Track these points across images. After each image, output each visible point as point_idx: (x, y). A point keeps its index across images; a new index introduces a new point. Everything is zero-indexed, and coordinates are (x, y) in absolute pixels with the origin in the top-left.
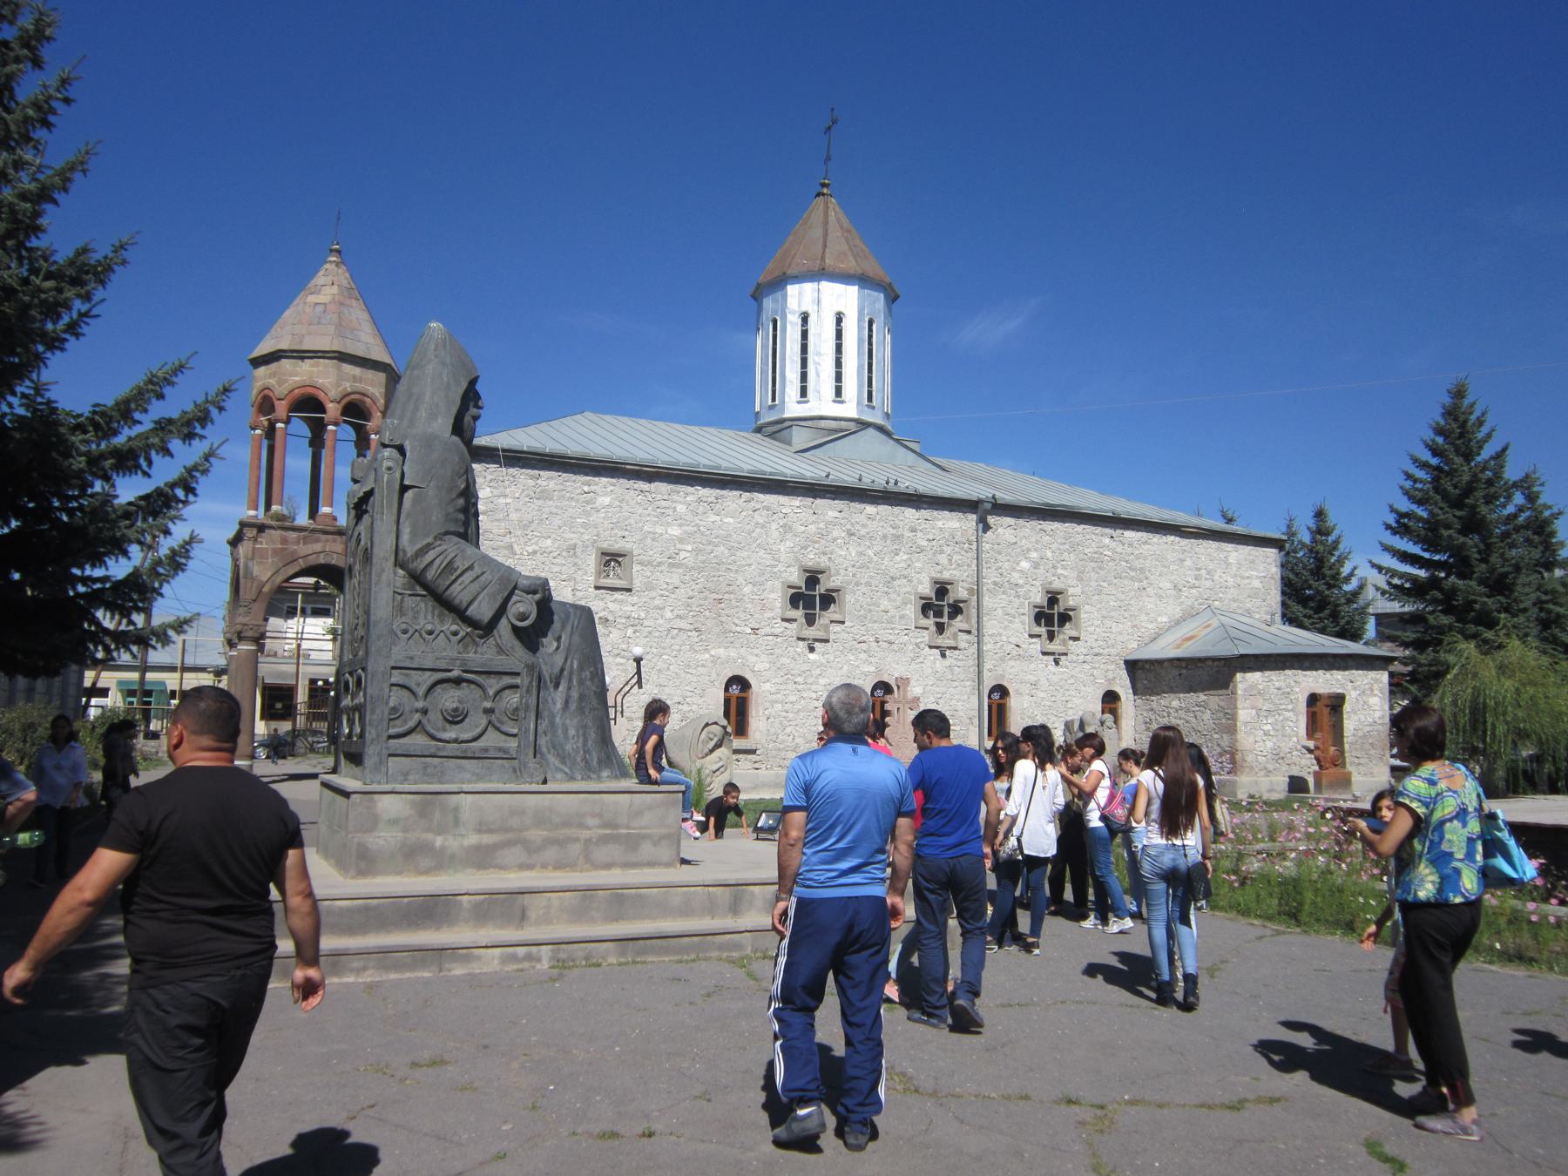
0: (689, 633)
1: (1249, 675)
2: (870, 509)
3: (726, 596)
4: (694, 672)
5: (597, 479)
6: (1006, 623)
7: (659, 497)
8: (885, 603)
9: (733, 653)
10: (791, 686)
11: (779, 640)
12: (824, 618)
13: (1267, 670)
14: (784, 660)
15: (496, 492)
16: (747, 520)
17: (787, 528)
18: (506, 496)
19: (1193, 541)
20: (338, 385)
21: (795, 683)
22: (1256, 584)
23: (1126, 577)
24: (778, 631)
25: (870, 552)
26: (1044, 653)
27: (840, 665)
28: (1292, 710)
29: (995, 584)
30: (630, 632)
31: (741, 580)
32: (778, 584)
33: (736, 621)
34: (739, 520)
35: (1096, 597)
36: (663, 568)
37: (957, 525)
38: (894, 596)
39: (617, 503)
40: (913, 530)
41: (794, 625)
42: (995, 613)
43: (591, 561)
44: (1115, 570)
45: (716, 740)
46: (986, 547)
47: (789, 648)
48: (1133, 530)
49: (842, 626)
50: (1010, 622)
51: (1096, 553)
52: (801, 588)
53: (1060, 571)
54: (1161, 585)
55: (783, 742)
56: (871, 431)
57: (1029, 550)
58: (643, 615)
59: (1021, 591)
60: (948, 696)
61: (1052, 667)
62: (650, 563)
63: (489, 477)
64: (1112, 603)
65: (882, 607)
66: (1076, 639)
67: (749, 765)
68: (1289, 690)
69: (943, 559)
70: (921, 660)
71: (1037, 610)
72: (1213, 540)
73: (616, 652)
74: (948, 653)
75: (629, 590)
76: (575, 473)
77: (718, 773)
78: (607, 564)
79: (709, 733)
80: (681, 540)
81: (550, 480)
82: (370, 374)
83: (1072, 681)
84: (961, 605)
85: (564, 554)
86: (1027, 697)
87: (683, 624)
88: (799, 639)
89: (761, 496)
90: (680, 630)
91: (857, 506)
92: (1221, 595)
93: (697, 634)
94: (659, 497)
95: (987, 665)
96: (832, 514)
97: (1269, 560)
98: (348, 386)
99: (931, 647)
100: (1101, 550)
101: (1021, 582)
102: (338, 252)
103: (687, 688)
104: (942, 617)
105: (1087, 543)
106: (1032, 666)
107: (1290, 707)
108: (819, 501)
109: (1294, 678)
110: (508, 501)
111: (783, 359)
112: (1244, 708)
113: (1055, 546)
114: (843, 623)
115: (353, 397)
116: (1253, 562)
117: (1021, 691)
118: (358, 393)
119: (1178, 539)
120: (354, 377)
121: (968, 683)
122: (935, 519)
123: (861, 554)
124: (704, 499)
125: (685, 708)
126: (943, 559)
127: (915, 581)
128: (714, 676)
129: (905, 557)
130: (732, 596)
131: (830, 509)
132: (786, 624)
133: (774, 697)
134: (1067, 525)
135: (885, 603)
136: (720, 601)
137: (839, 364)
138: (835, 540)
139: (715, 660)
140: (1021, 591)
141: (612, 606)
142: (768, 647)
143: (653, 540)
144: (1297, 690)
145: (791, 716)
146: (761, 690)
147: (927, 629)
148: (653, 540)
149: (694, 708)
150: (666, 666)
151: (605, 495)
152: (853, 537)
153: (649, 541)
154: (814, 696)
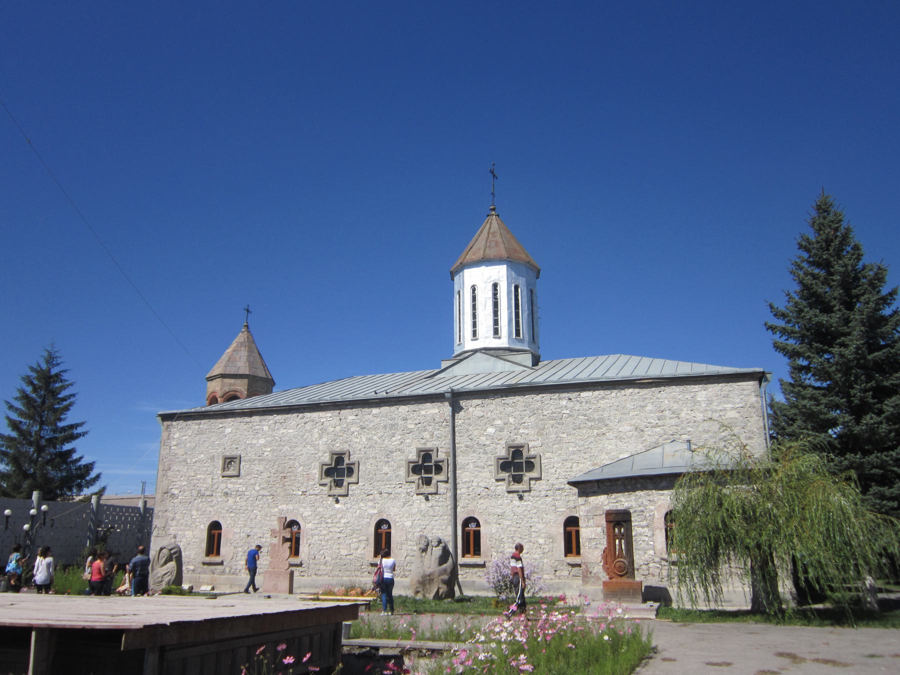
0: (268, 497)
1: (592, 499)
2: (375, 411)
3: (288, 474)
5: (225, 420)
6: (476, 473)
7: (255, 424)
8: (386, 469)
9: (291, 507)
10: (324, 525)
12: (347, 480)
13: (613, 493)
14: (321, 509)
15: (182, 434)
16: (301, 430)
17: (323, 431)
18: (185, 436)
19: (653, 389)
20: (221, 389)
21: (327, 523)
22: (732, 414)
23: (584, 427)
24: (316, 492)
25: (375, 438)
26: (509, 492)
27: (354, 511)
28: (647, 526)
29: (467, 446)
30: (238, 498)
31: (297, 464)
33: (293, 488)
34: (296, 430)
35: (555, 446)
36: (256, 462)
37: (437, 411)
38: (393, 463)
39: (234, 431)
40: (405, 419)
41: (326, 488)
42: (467, 467)
43: (220, 463)
46: (458, 422)
47: (324, 502)
48: (590, 390)
49: (357, 486)
50: (480, 472)
51: (555, 413)
52: (331, 465)
53: (521, 431)
54: (620, 429)
55: (318, 559)
56: (478, 354)
57: (494, 419)
59: (488, 449)
60: (430, 527)
61: (517, 502)
62: (249, 461)
63: (179, 427)
64: (570, 449)
65: (384, 471)
66: (540, 479)
68: (642, 508)
69: (426, 435)
70: (410, 503)
71: (501, 461)
72: (677, 385)
73: (230, 510)
74: (430, 497)
75: (238, 476)
76: (216, 419)
77: (166, 576)
78: (230, 463)
80: (265, 446)
81: (205, 424)
82: (238, 381)
83: (535, 511)
84: (441, 464)
85: (209, 461)
86: (495, 525)
87: (266, 493)
88: (330, 496)
89: (308, 415)
90: (263, 496)
91: (366, 410)
92: (690, 429)
93: (271, 497)
94: (255, 424)
95: (460, 504)
96: (351, 418)
97: (745, 392)
98: (227, 389)
99: (418, 494)
100: (560, 410)
101: (488, 443)
102: (247, 326)
104: (431, 473)
106: (500, 502)
107: (644, 523)
108: (343, 412)
109: (648, 498)
110: (187, 437)
111: (463, 319)
112: (587, 526)
113: (517, 413)
114: (357, 483)
115: (230, 393)
116: (727, 396)
117: (490, 521)
118: (232, 391)
119: (637, 390)
120: (230, 385)
121: (446, 517)
123: (369, 439)
124: (278, 421)
127: (406, 451)
129: (399, 437)
130: (292, 474)
131: (349, 415)
132: (321, 488)
133: (313, 532)
134: (526, 397)
135: (386, 469)
136: (285, 477)
137: (496, 313)
138: (353, 433)
140: (488, 449)
141: (230, 486)
142: (311, 502)
143: (251, 447)
144: (652, 508)
145: (323, 543)
146: (306, 527)
147: (414, 482)
148: (251, 447)
150: (255, 516)
151: (229, 428)
153: (249, 448)
154: (338, 530)
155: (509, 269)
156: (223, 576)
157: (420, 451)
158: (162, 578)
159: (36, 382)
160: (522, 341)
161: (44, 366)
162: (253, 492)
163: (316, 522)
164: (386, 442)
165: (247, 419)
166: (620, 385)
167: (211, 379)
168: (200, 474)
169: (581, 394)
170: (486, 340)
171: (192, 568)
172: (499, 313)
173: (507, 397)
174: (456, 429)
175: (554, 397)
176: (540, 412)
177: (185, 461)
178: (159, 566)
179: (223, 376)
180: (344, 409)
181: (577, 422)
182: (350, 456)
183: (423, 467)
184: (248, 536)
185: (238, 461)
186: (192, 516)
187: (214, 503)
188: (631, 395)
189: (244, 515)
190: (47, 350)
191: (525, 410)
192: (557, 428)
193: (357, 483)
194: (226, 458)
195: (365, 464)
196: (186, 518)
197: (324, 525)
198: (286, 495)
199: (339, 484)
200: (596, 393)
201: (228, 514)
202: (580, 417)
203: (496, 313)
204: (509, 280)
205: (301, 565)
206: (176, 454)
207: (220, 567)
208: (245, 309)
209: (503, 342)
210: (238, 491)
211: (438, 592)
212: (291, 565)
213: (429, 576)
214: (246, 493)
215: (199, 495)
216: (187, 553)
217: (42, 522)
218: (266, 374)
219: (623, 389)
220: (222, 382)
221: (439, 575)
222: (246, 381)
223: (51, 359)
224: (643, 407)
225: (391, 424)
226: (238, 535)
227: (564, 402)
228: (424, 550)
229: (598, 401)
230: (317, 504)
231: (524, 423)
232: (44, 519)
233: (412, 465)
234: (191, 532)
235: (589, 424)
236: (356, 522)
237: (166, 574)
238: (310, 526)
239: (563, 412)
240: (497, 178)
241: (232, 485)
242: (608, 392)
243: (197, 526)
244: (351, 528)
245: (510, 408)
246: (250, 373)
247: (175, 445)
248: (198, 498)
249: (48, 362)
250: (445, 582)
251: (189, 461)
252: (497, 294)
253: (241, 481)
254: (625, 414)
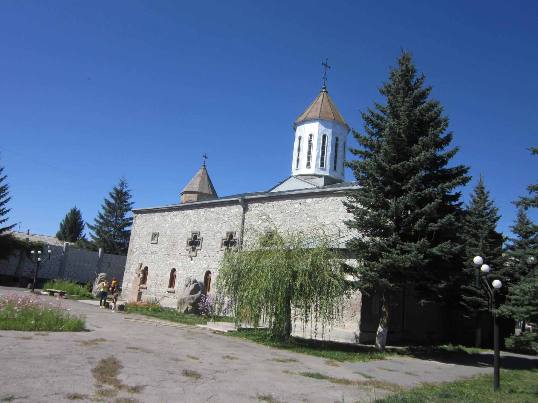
2: (212, 210)
3: (175, 244)
4: (165, 267)
7: (166, 216)
8: (213, 243)
11: (185, 257)
20: (184, 200)
23: (305, 221)
31: (179, 238)
32: (186, 239)
33: (176, 251)
36: (164, 236)
41: (188, 252)
43: (151, 236)
44: (300, 218)
46: (247, 217)
48: (311, 198)
51: (292, 212)
52: (191, 239)
67: (172, 297)
69: (232, 224)
75: (157, 243)
89: (185, 211)
90: (165, 255)
91: (209, 209)
93: (167, 256)
100: (294, 210)
102: (204, 166)
105: (288, 209)
113: (274, 212)
114: (201, 250)
119: (336, 198)
120: (189, 197)
122: (231, 209)
123: (208, 226)
126: (232, 224)
129: (220, 225)
132: (187, 251)
135: (213, 243)
138: (202, 222)
139: (170, 264)
141: (153, 249)
147: (223, 251)
152: (207, 220)
155: (321, 125)
156: (146, 295)
157: (228, 233)
159: (114, 195)
160: (325, 170)
161: (119, 188)
163: (182, 270)
164: (215, 227)
165: (163, 214)
166: (327, 194)
167: (182, 194)
168: (144, 242)
169: (306, 200)
170: (304, 170)
172: (311, 153)
173: (270, 202)
174: (245, 221)
175: (293, 202)
176: (285, 211)
177: (139, 235)
179: (186, 192)
180: (200, 208)
181: (303, 218)
182: (199, 234)
183: (230, 243)
185: (157, 235)
188: (332, 201)
190: (121, 180)
191: (277, 210)
192: (292, 221)
193: (201, 250)
194: (153, 234)
195: (205, 239)
197: (185, 272)
198: (173, 255)
199: (194, 250)
200: (314, 199)
202: (304, 215)
203: (309, 153)
204: (320, 132)
205: (174, 292)
206: (137, 231)
207: (145, 290)
208: (203, 156)
209: (312, 171)
210: (156, 251)
211: (187, 309)
212: (140, 288)
213: (183, 299)
217: (48, 258)
218: (209, 192)
219: (328, 197)
220: (185, 196)
221: (188, 300)
222: (196, 195)
223: (123, 184)
224: (338, 209)
225: (218, 217)
226: (153, 275)
227: (297, 205)
228: (187, 286)
229: (314, 205)
230: (184, 260)
231: (276, 218)
232: (49, 256)
233: (224, 241)
235: (308, 219)
236: (198, 272)
237: (98, 288)
238: (180, 272)
239: (296, 211)
240: (330, 68)
241: (155, 248)
242: (320, 199)
244: (195, 274)
245: (271, 209)
246: (199, 191)
247: (137, 227)
249: (121, 186)
250: (191, 304)
251: (140, 235)
252: (311, 141)
253: (157, 246)
254: (327, 213)
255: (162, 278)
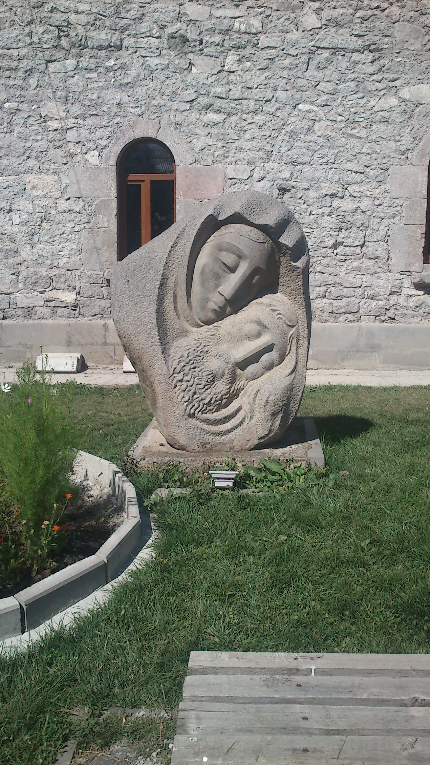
0: (356, 57)
4: (363, 133)
30: (231, 59)
45: (243, 269)
58: (256, 24)
73: (204, 101)
77: (252, 369)
79: (220, 248)
90: (335, 50)
93: (370, 57)
103: (349, 166)
125: (347, 205)
128: (406, 141)
149: (365, 204)
150: (306, 124)
158: (233, 380)
162: (294, 36)
171: (70, 297)
178: (197, 314)
184: (283, 190)
186: (45, 119)
187: (133, 72)
189: (259, 118)
196: (17, 129)
201: (194, 116)
214: (264, 41)
215: (64, 42)
216: (43, 249)
234: (49, 179)
237: (255, 358)
243: (72, 155)
248: (60, 54)
255: (347, 205)
